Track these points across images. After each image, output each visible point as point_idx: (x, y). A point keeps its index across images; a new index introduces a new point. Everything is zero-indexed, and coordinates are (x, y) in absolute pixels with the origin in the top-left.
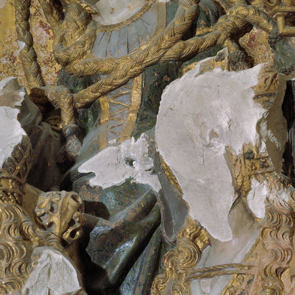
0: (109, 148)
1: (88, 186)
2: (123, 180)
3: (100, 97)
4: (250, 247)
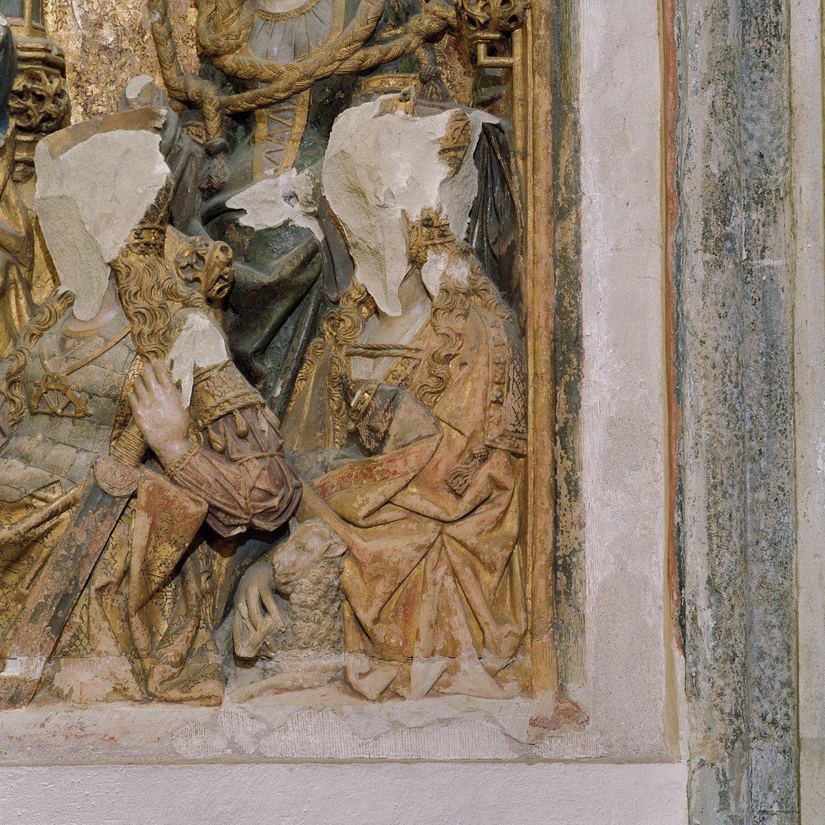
0: (264, 181)
1: (237, 225)
2: (280, 222)
3: (256, 108)
4: (420, 327)
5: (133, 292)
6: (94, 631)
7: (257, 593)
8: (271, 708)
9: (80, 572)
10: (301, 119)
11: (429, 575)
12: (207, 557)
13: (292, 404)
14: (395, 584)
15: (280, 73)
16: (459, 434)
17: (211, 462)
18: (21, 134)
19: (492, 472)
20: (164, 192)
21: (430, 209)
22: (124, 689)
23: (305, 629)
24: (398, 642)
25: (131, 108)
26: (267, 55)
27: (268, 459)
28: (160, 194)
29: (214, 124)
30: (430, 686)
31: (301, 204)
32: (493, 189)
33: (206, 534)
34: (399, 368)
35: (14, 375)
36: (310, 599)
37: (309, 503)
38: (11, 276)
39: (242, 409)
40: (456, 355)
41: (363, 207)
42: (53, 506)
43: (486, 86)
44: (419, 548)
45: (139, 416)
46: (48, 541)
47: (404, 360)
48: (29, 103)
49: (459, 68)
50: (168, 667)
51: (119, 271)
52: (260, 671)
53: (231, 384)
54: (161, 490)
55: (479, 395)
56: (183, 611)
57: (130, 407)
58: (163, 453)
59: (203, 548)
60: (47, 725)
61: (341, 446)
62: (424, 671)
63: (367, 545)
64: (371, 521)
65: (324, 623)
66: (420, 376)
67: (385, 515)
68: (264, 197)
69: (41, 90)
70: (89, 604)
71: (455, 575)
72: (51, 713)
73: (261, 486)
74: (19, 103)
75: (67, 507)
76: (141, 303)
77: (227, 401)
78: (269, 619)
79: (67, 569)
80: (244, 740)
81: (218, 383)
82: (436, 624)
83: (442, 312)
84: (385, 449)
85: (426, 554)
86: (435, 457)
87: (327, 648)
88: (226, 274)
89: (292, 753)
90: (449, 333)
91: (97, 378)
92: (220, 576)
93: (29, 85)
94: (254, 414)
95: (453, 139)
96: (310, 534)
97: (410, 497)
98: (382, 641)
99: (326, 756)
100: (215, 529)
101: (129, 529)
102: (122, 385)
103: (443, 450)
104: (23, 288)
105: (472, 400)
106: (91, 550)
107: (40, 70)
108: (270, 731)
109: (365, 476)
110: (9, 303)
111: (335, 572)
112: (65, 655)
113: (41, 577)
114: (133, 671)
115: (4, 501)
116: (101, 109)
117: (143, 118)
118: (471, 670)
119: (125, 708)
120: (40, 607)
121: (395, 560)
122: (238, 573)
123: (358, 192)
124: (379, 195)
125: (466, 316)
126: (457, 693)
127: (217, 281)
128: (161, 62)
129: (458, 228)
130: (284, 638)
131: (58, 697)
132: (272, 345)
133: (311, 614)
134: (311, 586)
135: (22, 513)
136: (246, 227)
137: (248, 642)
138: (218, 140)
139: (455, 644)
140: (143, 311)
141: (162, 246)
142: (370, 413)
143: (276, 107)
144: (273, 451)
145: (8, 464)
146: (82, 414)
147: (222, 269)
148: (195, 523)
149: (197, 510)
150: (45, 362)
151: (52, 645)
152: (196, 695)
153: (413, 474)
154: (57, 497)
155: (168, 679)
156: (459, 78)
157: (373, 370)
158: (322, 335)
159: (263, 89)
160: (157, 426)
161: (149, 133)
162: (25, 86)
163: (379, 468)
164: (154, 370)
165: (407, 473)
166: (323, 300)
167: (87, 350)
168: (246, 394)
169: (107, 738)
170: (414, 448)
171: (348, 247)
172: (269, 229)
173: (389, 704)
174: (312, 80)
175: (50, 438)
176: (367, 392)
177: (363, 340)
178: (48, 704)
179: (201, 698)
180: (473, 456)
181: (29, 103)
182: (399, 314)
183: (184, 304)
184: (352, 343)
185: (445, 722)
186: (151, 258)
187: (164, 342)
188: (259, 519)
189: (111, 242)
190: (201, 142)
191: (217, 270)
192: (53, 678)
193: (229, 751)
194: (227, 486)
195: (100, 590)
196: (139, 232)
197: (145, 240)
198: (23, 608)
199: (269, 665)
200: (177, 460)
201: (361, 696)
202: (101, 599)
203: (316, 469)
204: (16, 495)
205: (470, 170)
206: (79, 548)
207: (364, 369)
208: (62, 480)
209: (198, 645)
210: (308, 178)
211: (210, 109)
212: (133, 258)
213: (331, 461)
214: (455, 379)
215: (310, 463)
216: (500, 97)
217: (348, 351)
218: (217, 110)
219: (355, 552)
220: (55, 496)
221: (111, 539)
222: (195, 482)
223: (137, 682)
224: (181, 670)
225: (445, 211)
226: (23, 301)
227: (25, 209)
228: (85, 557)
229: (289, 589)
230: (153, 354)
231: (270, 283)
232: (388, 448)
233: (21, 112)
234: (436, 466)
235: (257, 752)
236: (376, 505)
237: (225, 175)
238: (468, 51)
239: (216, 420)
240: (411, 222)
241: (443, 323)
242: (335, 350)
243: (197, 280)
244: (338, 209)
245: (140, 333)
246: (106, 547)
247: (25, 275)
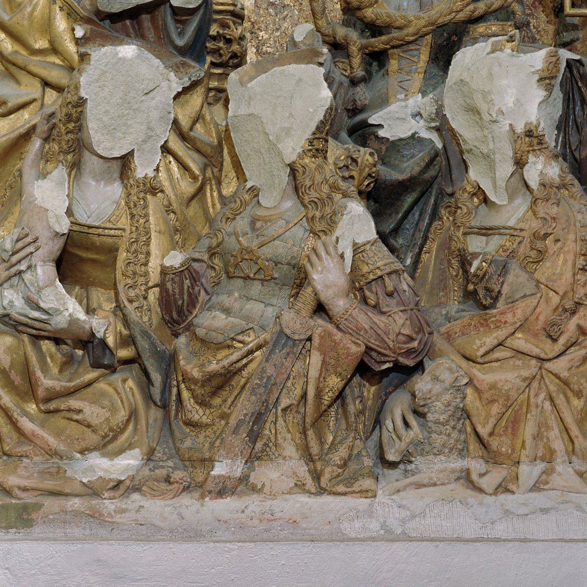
0: (398, 103)
1: (377, 137)
2: (409, 134)
3: (390, 49)
4: (523, 212)
5: (308, 186)
6: (280, 441)
7: (400, 412)
8: (413, 499)
9: (269, 397)
10: (424, 56)
11: (532, 400)
12: (360, 386)
13: (419, 271)
14: (506, 406)
15: (410, 22)
16: (554, 294)
17: (367, 314)
18: (214, 68)
19: (580, 322)
20: (329, 111)
21: (531, 123)
22: (303, 484)
23: (438, 440)
24: (507, 450)
25: (298, 48)
26: (399, 8)
27: (409, 312)
28: (326, 112)
29: (357, 61)
30: (533, 484)
31: (425, 121)
32: (574, 108)
33: (363, 369)
34: (508, 244)
35: (214, 248)
36: (442, 418)
37: (439, 345)
38: (207, 175)
39: (389, 274)
40: (551, 234)
41: (477, 123)
42: (250, 346)
43: (567, 31)
44: (525, 379)
45: (313, 279)
46: (245, 373)
47: (512, 237)
48: (221, 44)
49: (542, 16)
50: (335, 468)
51: (297, 170)
52: (402, 472)
53: (380, 255)
54: (330, 335)
55: (570, 263)
56: (344, 426)
57: (306, 273)
58: (331, 307)
59: (357, 379)
60: (246, 511)
61: (459, 303)
62: (529, 472)
63: (484, 377)
64: (487, 359)
65: (453, 435)
66: (524, 249)
67: (497, 355)
68: (397, 116)
69: (230, 35)
70: (276, 420)
71: (551, 399)
72: (249, 502)
73: (405, 332)
74: (214, 44)
75: (259, 347)
76: (313, 194)
77: (378, 268)
78: (411, 432)
79: (260, 394)
80: (393, 524)
81: (371, 254)
82: (537, 437)
83: (541, 201)
84: (498, 305)
85: (530, 384)
86: (536, 311)
87: (455, 454)
88: (373, 173)
89: (430, 534)
90: (547, 217)
91: (281, 251)
92: (368, 399)
93: (221, 32)
94: (398, 278)
95: (548, 70)
96: (442, 368)
97: (517, 340)
98: (495, 449)
99: (455, 536)
100: (369, 364)
101: (305, 364)
102: (299, 256)
103: (543, 305)
104: (216, 184)
105: (564, 268)
106: (278, 380)
107: (229, 19)
108: (413, 517)
109: (482, 325)
110: (206, 195)
111: (461, 398)
112: (259, 458)
113: (241, 400)
114: (309, 471)
115: (212, 343)
116: (269, 50)
117: (310, 56)
118: (564, 473)
119: (304, 499)
120: (240, 423)
121: (506, 388)
122: (384, 398)
123: (473, 110)
124: (492, 113)
125: (558, 205)
126: (553, 489)
127: (366, 178)
128: (314, 14)
129: (550, 138)
130: (422, 447)
131: (253, 490)
132: (402, 227)
133: (443, 429)
134: (443, 408)
135: (225, 352)
136: (383, 138)
137: (394, 450)
138: (360, 73)
139: (552, 452)
140: (316, 200)
141: (327, 152)
142: (487, 277)
143: (405, 48)
144: (412, 306)
145: (213, 315)
146: (269, 277)
147: (371, 169)
148: (356, 360)
149: (356, 350)
150: (240, 239)
151: (250, 451)
152: (357, 489)
153: (519, 324)
154: (251, 340)
155: (335, 478)
156: (543, 26)
157: (487, 245)
158: (441, 219)
159: (396, 34)
160: (327, 287)
161: (313, 67)
162: (218, 32)
163: (494, 319)
164: (324, 244)
165: (516, 323)
166: (441, 194)
167: (273, 230)
168: (392, 262)
169: (291, 521)
170: (521, 304)
171: (462, 152)
172: (401, 140)
173: (502, 497)
174: (435, 27)
175: (244, 296)
176: (484, 262)
177: (476, 222)
178: (246, 495)
179: (361, 492)
180: (565, 310)
181: (221, 44)
182: (506, 203)
183: (343, 195)
184: (468, 225)
185: (545, 511)
186: (319, 160)
187: (330, 223)
188: (402, 357)
189: (290, 148)
190: (347, 74)
191: (367, 169)
192: (249, 476)
193: (382, 532)
194: (379, 332)
195: (284, 410)
196: (312, 141)
197: (316, 147)
198: (227, 423)
199: (409, 467)
200: (341, 313)
201: (481, 490)
202: (285, 416)
203: (441, 320)
204: (220, 338)
205: (558, 94)
206: (269, 378)
207: (479, 244)
208: (255, 327)
209: (355, 452)
210: (432, 100)
211: (354, 49)
212: (307, 160)
213: (453, 313)
214: (551, 252)
215: (436, 315)
216: (578, 39)
217: (465, 231)
218: (359, 50)
219: (475, 382)
220: (250, 340)
221: (292, 372)
222: (355, 329)
223: (313, 478)
224: (344, 470)
225: (542, 125)
226: (215, 194)
227: (217, 125)
228: (273, 385)
229: (426, 410)
230: (323, 233)
231: (404, 180)
232: (501, 304)
233: (216, 52)
234: (537, 318)
235: (404, 533)
236: (491, 347)
237: (366, 99)
238: (551, 5)
239: (370, 282)
240: (517, 133)
241: (541, 209)
242: (454, 230)
243: (352, 177)
244: (458, 123)
245: (313, 216)
246: (288, 378)
247: (217, 174)
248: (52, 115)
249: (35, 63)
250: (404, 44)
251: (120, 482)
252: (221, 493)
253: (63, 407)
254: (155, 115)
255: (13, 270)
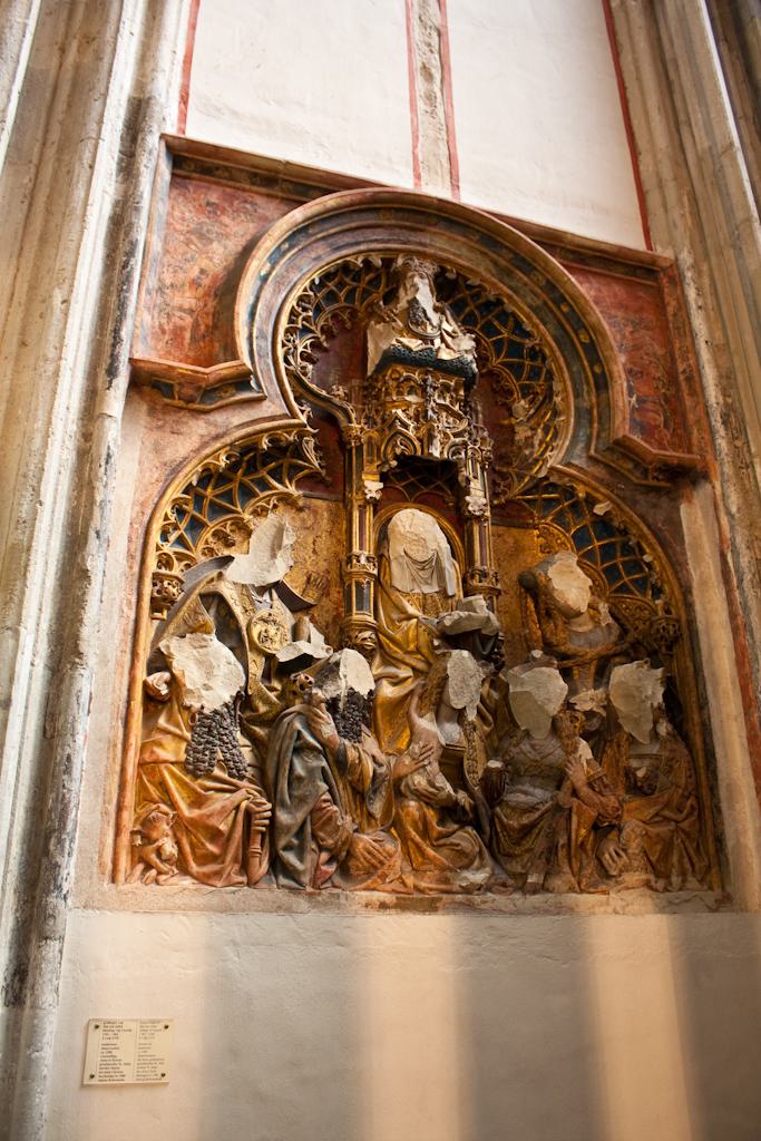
6: (561, 863)
23: (636, 864)
36: (637, 852)
67: (657, 819)
118: (692, 882)
154: (543, 808)
185: (687, 901)
195: (563, 846)
232: (657, 794)
244: (617, 703)
248: (424, 685)
249: (408, 659)
250: (582, 665)
251: (482, 885)
252: (535, 892)
253: (448, 842)
254: (474, 689)
255: (421, 764)
